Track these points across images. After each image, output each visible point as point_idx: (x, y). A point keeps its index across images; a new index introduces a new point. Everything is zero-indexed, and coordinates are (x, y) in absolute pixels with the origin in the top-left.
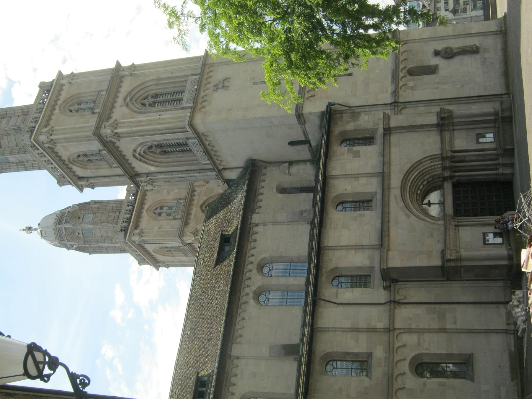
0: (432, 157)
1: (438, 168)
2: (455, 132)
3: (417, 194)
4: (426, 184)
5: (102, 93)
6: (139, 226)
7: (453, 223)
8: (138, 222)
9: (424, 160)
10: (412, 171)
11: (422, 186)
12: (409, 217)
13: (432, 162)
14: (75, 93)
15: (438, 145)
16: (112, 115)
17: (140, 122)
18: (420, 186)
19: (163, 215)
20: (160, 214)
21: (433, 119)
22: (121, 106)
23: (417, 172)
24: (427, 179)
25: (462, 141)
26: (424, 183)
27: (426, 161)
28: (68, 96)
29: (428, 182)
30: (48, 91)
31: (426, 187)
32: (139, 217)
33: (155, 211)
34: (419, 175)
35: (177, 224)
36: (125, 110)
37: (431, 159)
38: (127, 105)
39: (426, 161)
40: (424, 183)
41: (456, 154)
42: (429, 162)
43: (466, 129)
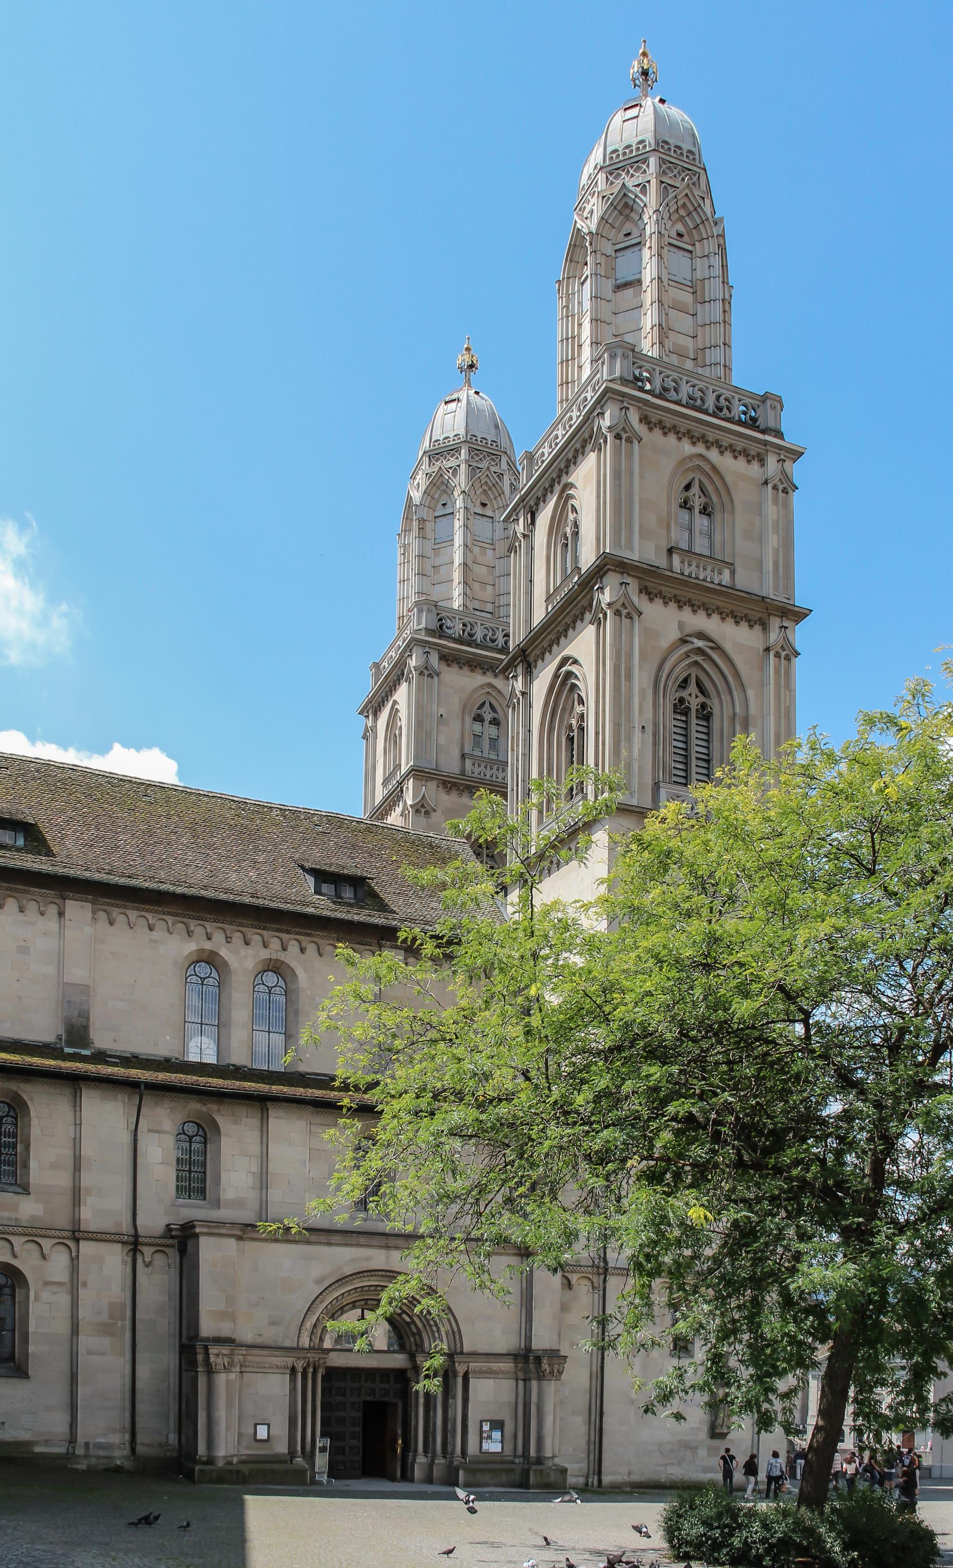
0: (457, 1334)
2: (513, 1382)
4: (403, 1319)
5: (727, 572)
6: (449, 665)
7: (300, 1365)
8: (458, 663)
14: (734, 495)
15: (483, 1347)
16: (659, 601)
17: (629, 677)
19: (477, 727)
20: (478, 718)
21: (542, 1340)
22: (681, 625)
25: (489, 1394)
26: (404, 1316)
28: (728, 479)
29: (408, 1324)
30: (753, 423)
31: (398, 1319)
32: (475, 664)
33: (487, 704)
35: (451, 765)
36: (674, 635)
37: (453, 1332)
38: (684, 641)
40: (404, 1316)
41: (460, 1380)
43: (516, 1403)
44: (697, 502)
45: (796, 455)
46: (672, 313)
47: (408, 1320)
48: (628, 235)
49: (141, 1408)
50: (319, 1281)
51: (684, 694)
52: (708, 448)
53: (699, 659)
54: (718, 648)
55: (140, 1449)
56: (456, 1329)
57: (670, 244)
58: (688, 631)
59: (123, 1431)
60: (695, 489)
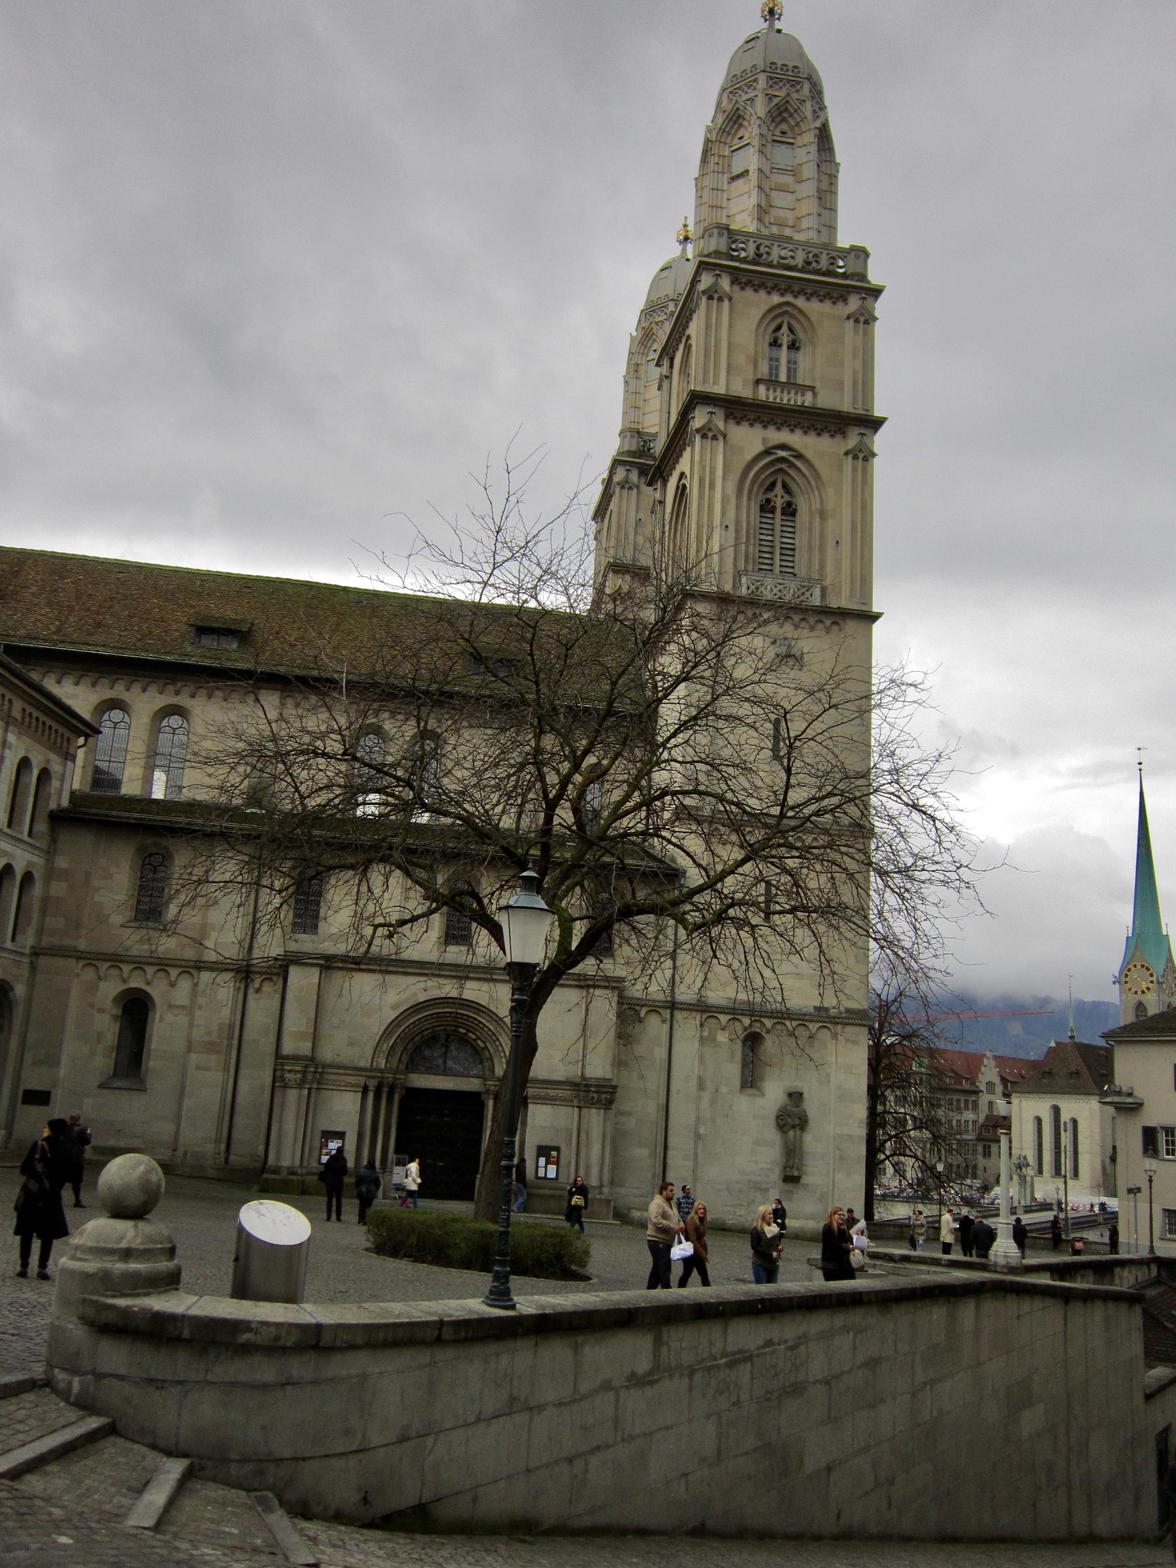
7: (372, 1084)
22: (764, 440)
24: (486, 1048)
28: (813, 319)
36: (758, 448)
38: (767, 452)
44: (785, 340)
45: (876, 292)
46: (774, 194)
47: (482, 1045)
48: (741, 138)
49: (238, 1119)
50: (394, 1007)
51: (770, 495)
52: (795, 297)
53: (784, 466)
54: (799, 456)
55: (232, 1158)
57: (774, 141)
58: (771, 444)
59: (217, 1141)
60: (785, 329)
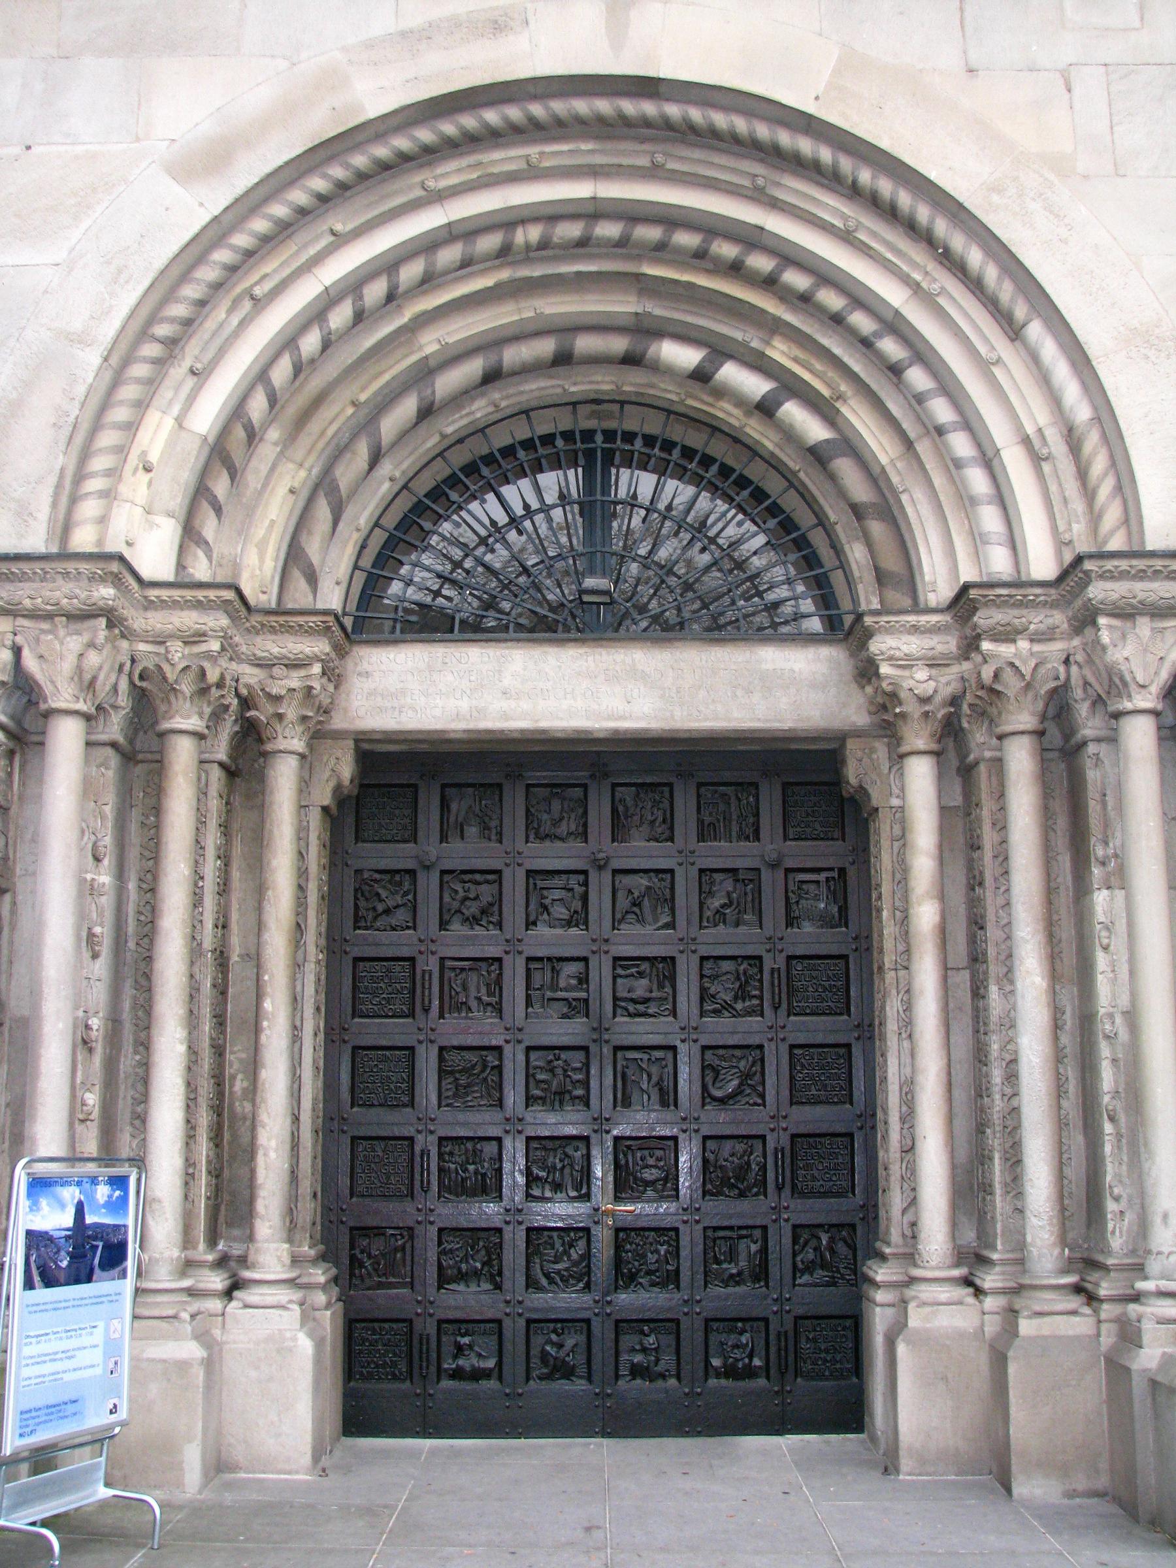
0: (1092, 441)
1: (978, 540)
3: (648, 330)
4: (789, 435)
9: (1049, 350)
10: (890, 213)
11: (755, 386)
12: (198, 164)
13: (1037, 459)
18: (759, 364)
23: (893, 294)
24: (849, 444)
27: (1044, 379)
29: (818, 455)
34: (861, 322)
39: (1044, 379)
42: (1036, 415)
47: (816, 431)
56: (1082, 413)
